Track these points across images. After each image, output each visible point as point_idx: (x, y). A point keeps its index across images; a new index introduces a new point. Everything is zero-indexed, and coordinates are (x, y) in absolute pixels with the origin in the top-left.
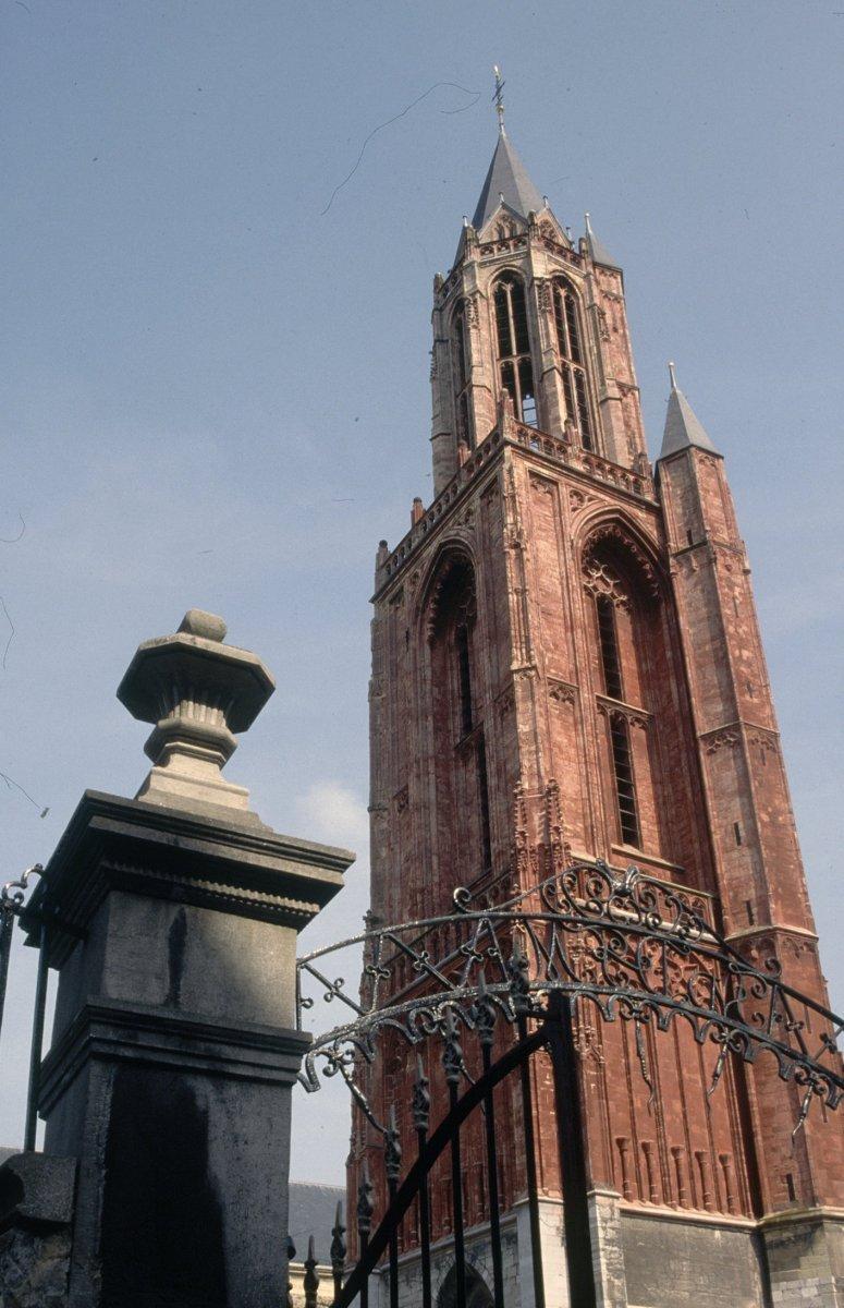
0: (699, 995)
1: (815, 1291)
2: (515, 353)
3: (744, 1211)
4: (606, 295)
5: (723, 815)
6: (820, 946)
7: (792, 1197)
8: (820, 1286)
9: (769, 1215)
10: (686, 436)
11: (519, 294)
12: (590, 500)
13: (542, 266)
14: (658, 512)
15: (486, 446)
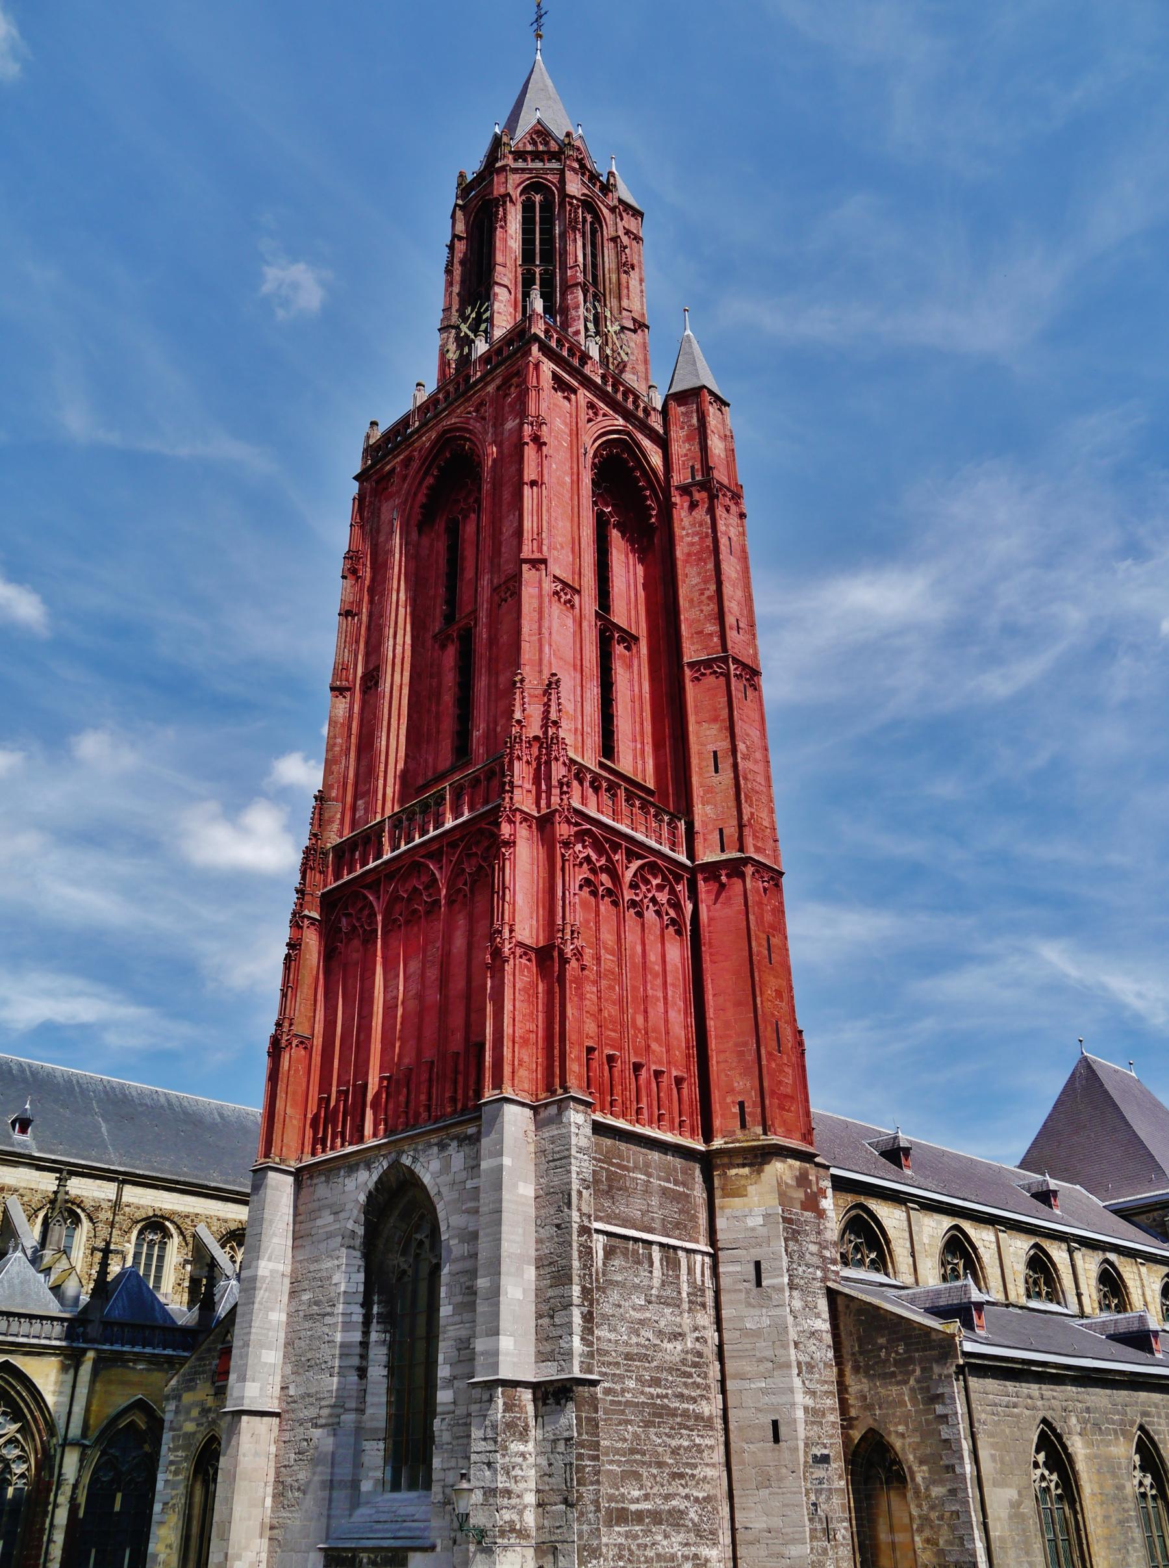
0: (667, 914)
1: (760, 1221)
2: (538, 263)
3: (693, 1134)
4: (627, 232)
5: (704, 737)
6: (784, 880)
7: (743, 1126)
8: (766, 1216)
9: (718, 1143)
10: (697, 376)
11: (547, 206)
12: (605, 415)
13: (575, 186)
14: (663, 443)
15: (508, 340)
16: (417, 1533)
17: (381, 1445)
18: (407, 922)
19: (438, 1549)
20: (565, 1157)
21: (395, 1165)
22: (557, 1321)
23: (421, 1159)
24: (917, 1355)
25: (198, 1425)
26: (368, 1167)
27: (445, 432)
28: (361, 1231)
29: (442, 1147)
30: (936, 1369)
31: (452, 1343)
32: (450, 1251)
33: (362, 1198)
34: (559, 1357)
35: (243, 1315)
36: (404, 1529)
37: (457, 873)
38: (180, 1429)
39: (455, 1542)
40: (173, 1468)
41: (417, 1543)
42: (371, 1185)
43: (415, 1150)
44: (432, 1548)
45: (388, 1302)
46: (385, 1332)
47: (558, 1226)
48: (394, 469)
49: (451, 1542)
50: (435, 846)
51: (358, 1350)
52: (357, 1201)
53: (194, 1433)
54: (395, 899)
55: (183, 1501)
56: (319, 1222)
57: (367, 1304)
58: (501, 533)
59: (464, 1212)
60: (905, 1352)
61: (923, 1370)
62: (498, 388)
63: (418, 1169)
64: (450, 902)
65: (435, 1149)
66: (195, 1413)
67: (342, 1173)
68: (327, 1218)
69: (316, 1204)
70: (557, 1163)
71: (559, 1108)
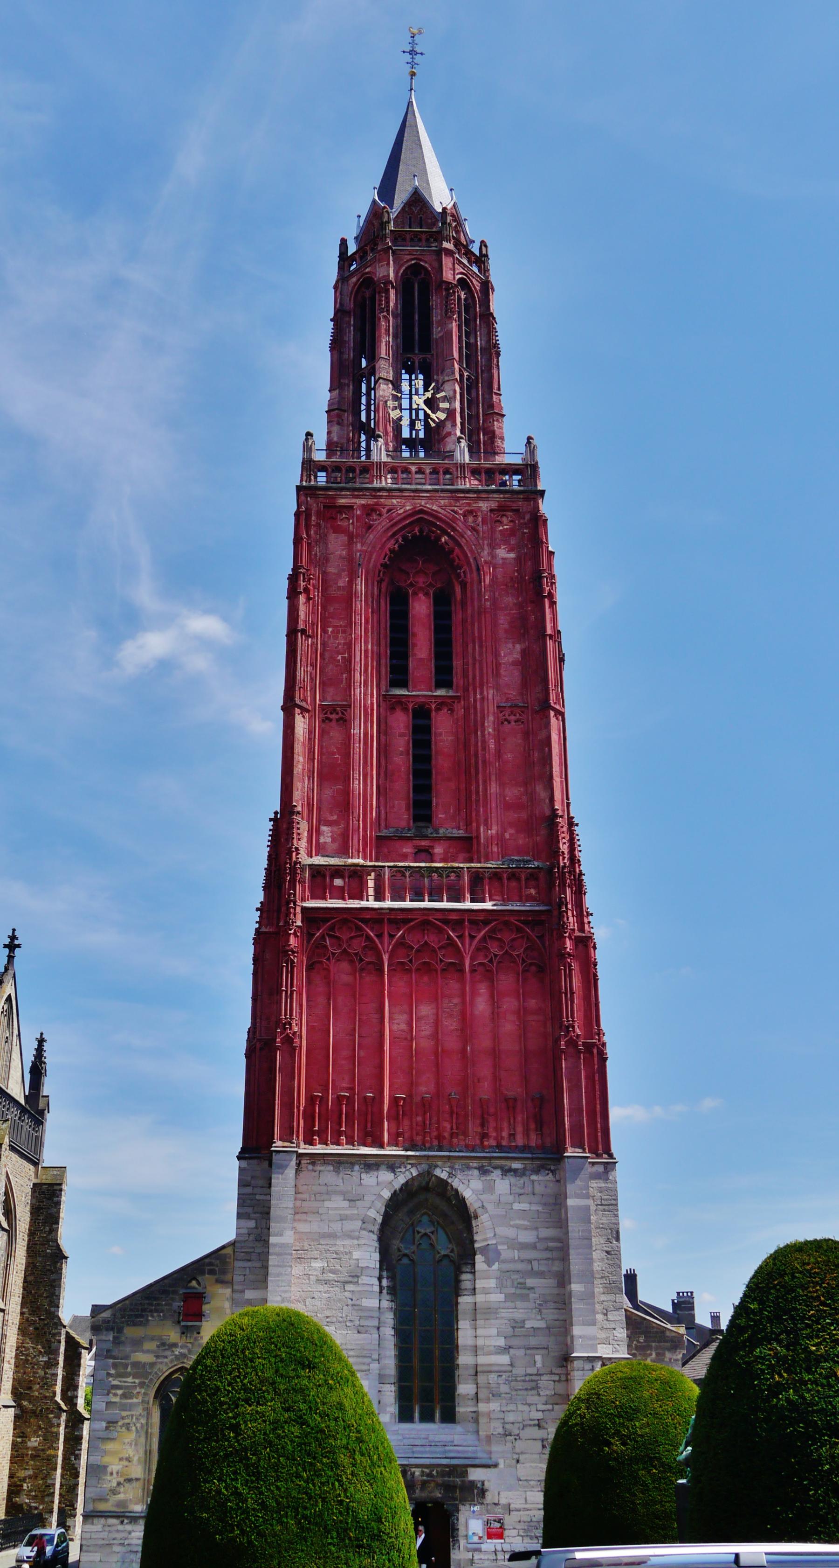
16: (469, 1455)
17: (393, 1388)
18: (418, 970)
19: (501, 1466)
20: (612, 1205)
21: (429, 1173)
22: (610, 1317)
23: (459, 1176)
24: (654, 1344)
25: (157, 1357)
26: (392, 1168)
27: (422, 511)
28: (380, 1219)
29: (483, 1171)
30: (668, 1355)
31: (506, 1321)
32: (499, 1253)
33: (387, 1194)
34: (614, 1342)
35: (279, 1275)
36: (450, 1451)
37: (481, 948)
38: (127, 1357)
39: (518, 1461)
40: (120, 1392)
41: (477, 1462)
42: (397, 1186)
43: (452, 1167)
44: (496, 1466)
45: (391, 1278)
46: (392, 1301)
47: (607, 1252)
48: (350, 508)
49: (514, 1462)
50: (454, 917)
51: (376, 1314)
52: (380, 1196)
53: (152, 1365)
54: (401, 943)
55: (143, 1421)
56: (327, 1204)
57: (380, 1279)
58: (500, 655)
59: (512, 1226)
60: (645, 1341)
61: (657, 1354)
62: (492, 510)
63: (455, 1183)
64: (473, 971)
65: (476, 1172)
66: (152, 1345)
67: (357, 1168)
68: (338, 1204)
69: (323, 1189)
70: (606, 1208)
71: (605, 1168)
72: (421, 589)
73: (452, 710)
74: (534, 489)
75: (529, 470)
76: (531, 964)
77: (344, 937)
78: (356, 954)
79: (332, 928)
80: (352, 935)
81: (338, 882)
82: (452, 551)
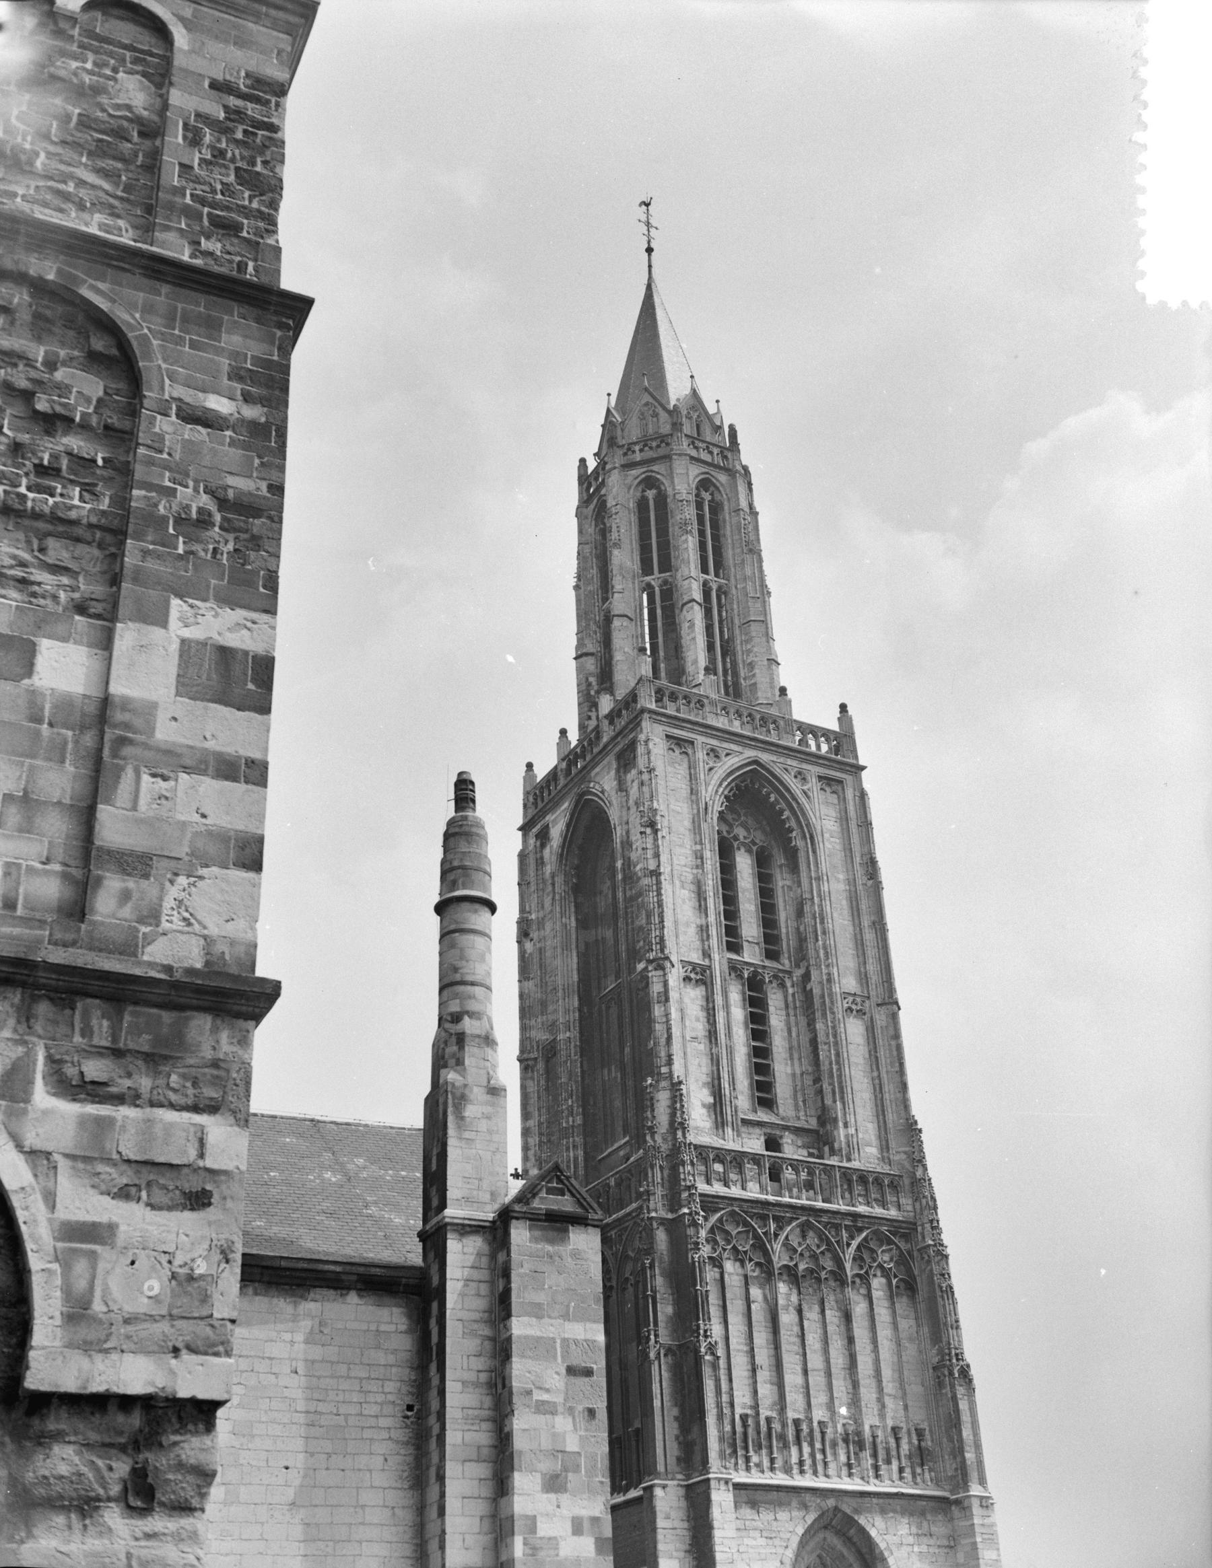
27: (756, 762)
56: (746, 1541)
63: (862, 1521)
72: (744, 844)
73: (782, 985)
74: (854, 762)
75: (843, 740)
76: (901, 1280)
77: (734, 1233)
78: (745, 1252)
79: (720, 1220)
80: (740, 1229)
81: (718, 1167)
82: (781, 812)
